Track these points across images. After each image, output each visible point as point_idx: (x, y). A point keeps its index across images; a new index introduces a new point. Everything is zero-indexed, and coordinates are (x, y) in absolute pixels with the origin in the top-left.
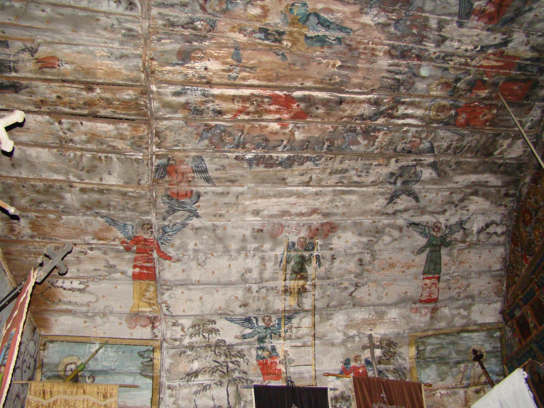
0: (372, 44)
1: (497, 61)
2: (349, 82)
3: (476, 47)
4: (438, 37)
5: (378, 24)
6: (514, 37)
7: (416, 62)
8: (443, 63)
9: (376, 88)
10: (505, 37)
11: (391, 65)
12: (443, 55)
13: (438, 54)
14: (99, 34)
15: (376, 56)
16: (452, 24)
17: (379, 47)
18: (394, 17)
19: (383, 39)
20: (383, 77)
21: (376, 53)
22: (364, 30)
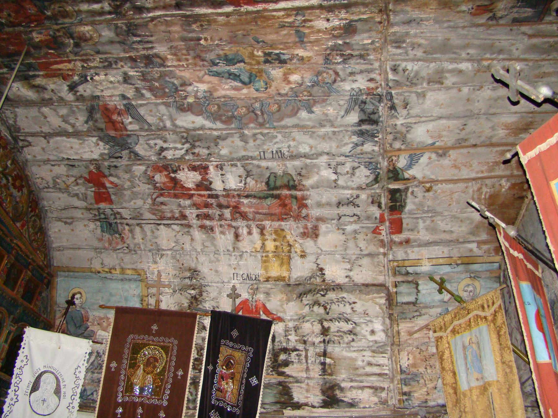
0: (183, 65)
1: (60, 70)
2: (182, 26)
3: (92, 79)
4: (133, 82)
5: (190, 85)
6: (70, 94)
7: (132, 54)
8: (106, 58)
9: (150, 24)
10: (78, 94)
11: (152, 48)
12: (114, 66)
13: (119, 66)
14: (426, 40)
15: (172, 54)
16: (131, 96)
17: (175, 63)
18: (182, 93)
19: (177, 71)
20: (152, 36)
21: (174, 57)
22: (198, 77)
